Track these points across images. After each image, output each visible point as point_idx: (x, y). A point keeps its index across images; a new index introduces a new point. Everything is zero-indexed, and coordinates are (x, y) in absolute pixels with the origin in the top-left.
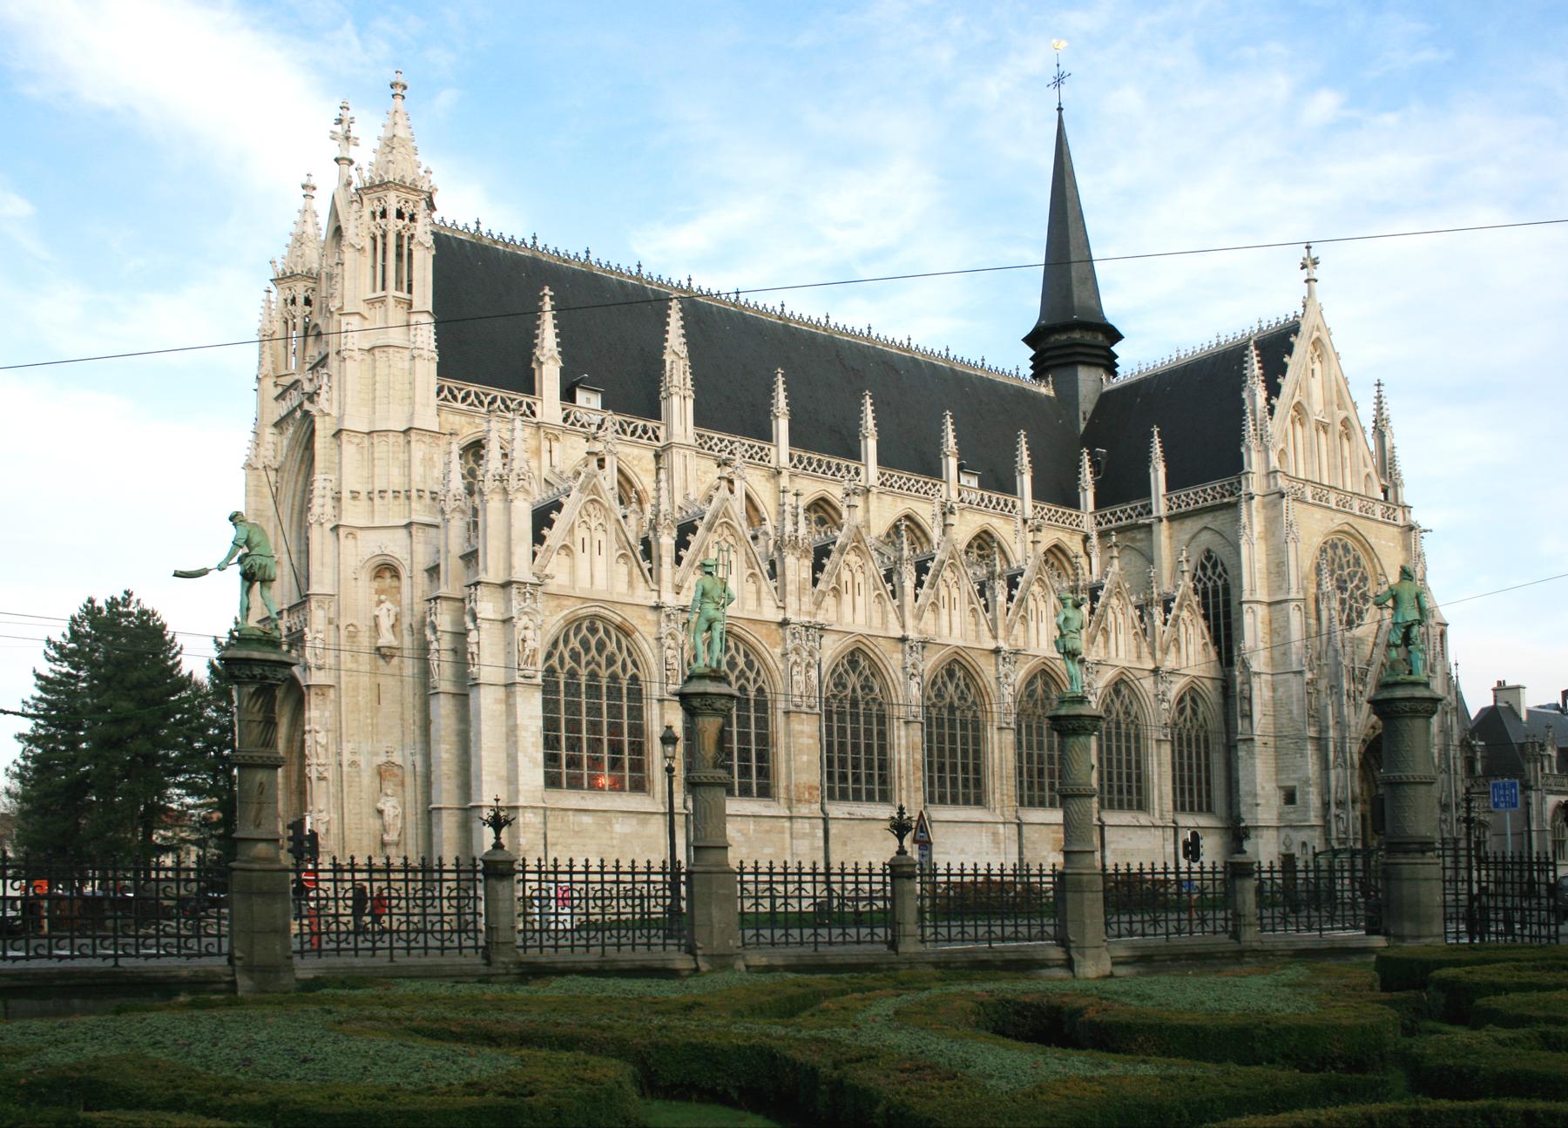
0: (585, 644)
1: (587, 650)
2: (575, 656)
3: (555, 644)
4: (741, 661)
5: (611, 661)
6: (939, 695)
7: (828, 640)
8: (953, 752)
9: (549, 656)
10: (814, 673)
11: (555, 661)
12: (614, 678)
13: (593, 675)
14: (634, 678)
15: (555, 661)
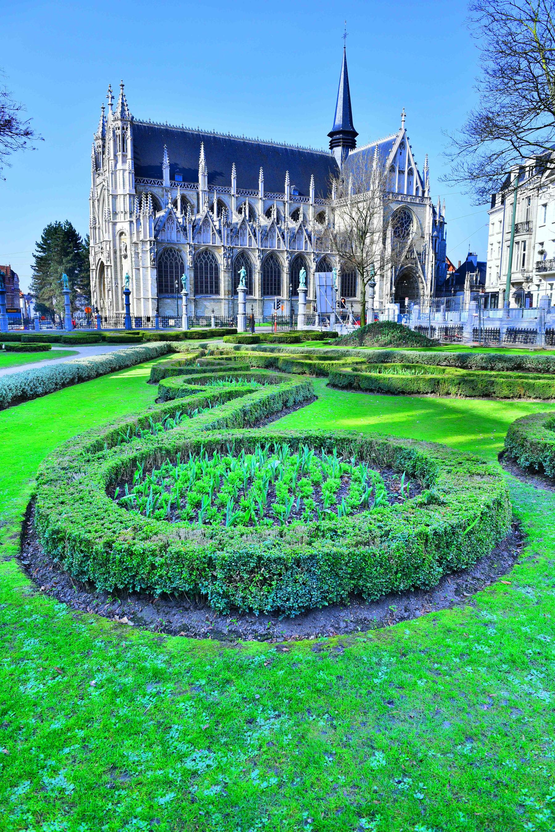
0: (169, 254)
1: (169, 256)
2: (166, 258)
3: (161, 256)
4: (211, 257)
5: (176, 259)
6: (268, 264)
7: (234, 250)
8: (271, 280)
9: (160, 258)
10: (229, 260)
11: (161, 260)
12: (177, 263)
13: (171, 263)
14: (182, 263)
15: (161, 260)
